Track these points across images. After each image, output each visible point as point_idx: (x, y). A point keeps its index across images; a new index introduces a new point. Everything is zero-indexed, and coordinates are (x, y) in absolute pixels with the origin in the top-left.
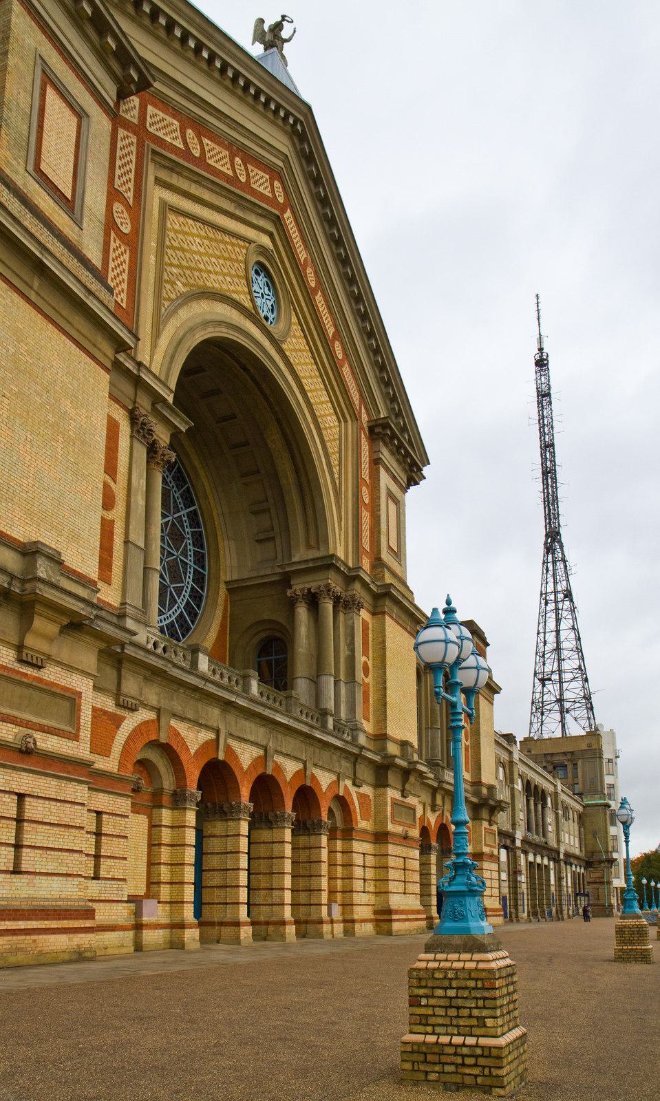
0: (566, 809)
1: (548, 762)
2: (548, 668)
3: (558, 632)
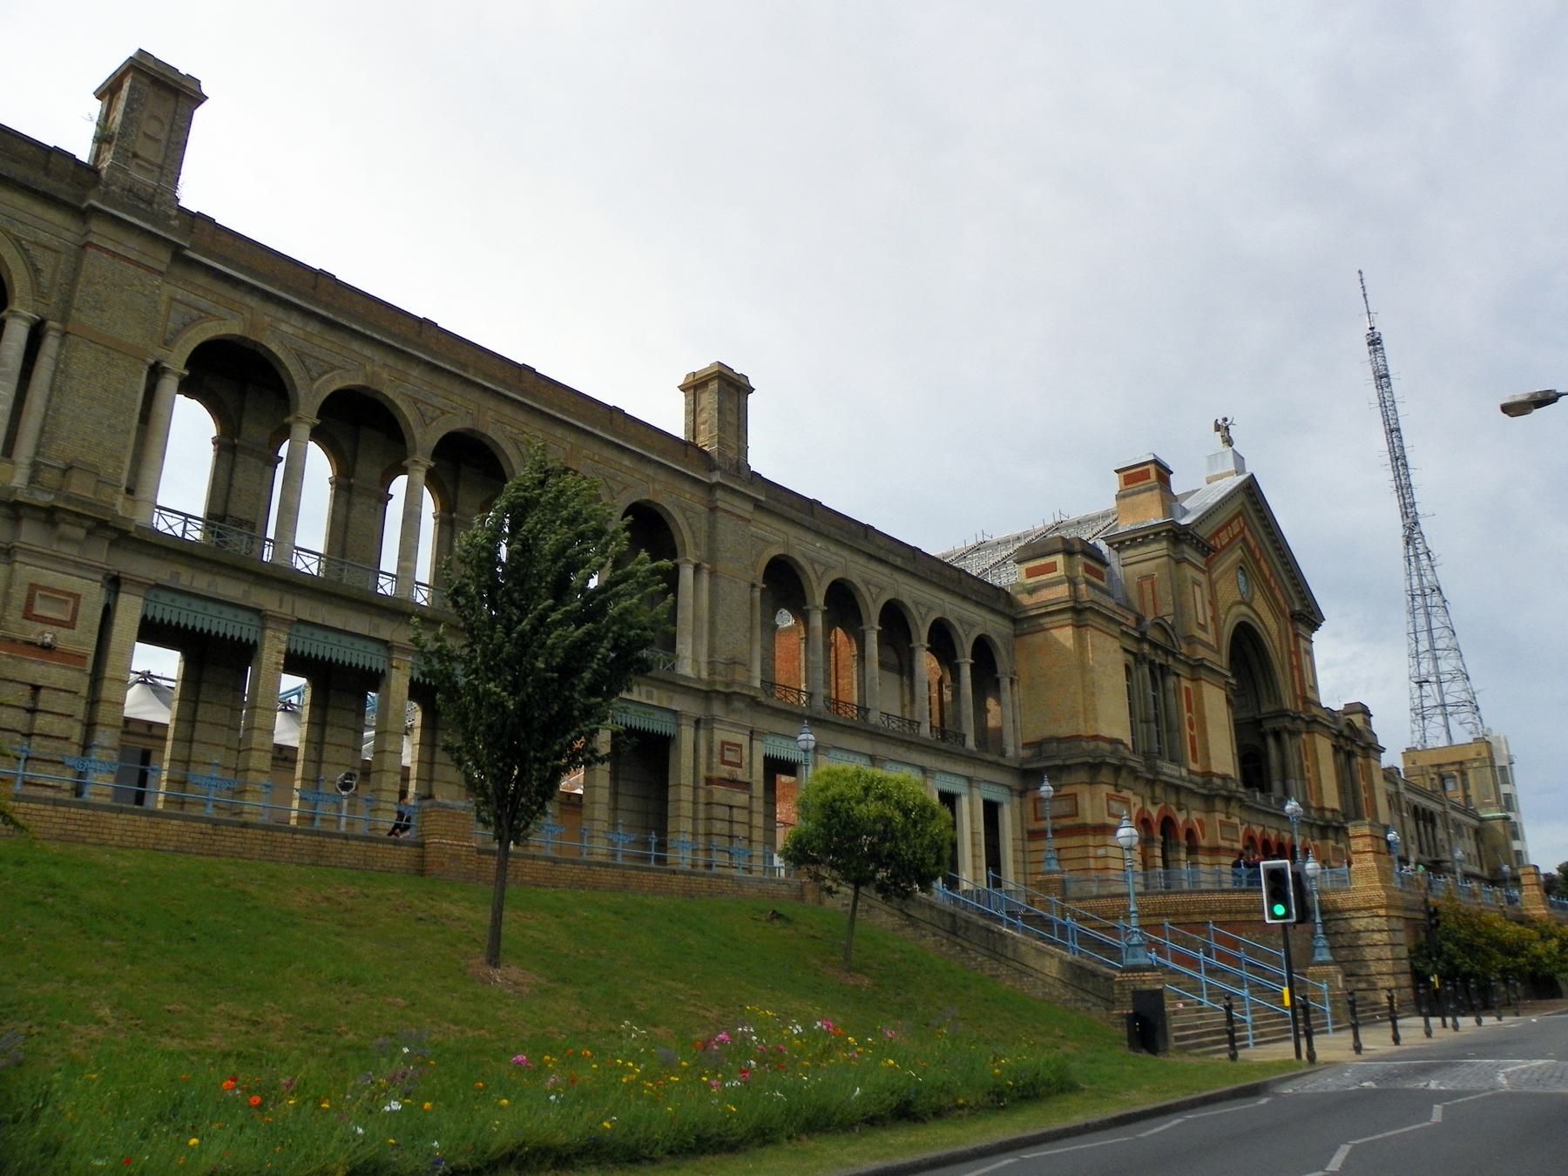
3: (1430, 630)
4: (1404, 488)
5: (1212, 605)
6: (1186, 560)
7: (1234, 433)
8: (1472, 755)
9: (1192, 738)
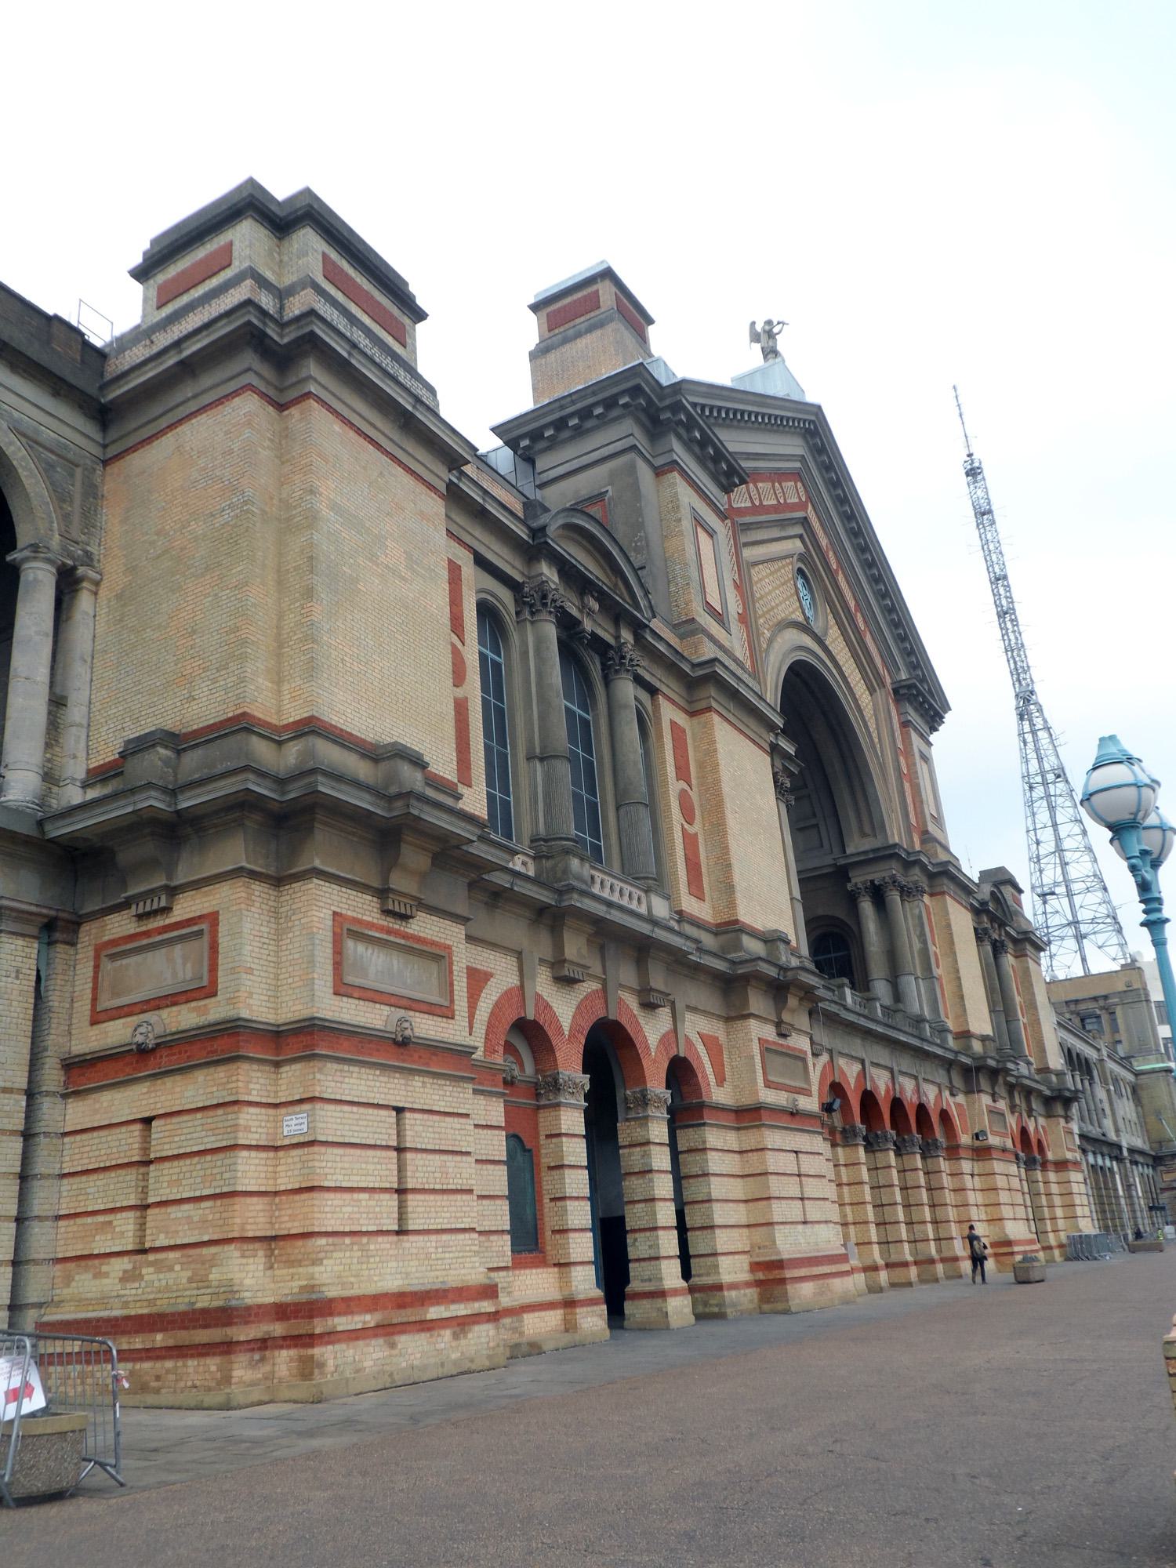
0: (1116, 1081)
1: (1072, 1013)
3: (1055, 825)
4: (1014, 650)
6: (673, 465)
7: (781, 344)
8: (1121, 987)
9: (690, 841)
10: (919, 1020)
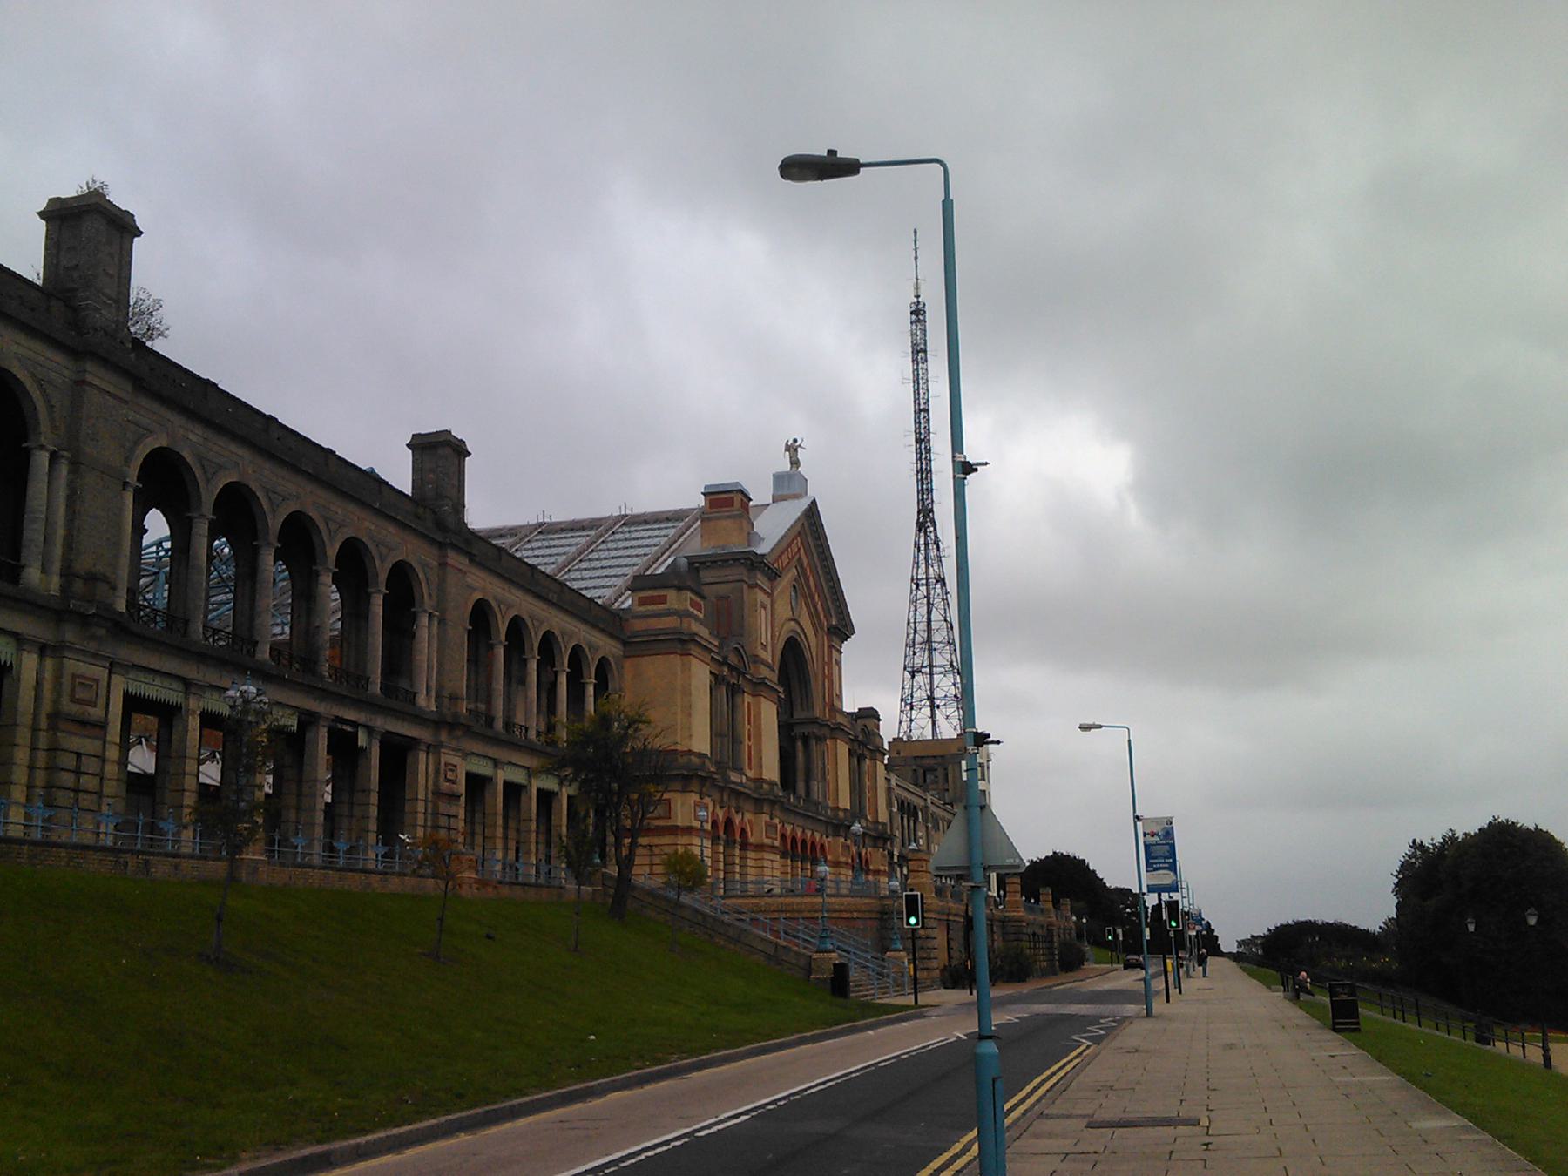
2: (918, 661)
5: (770, 620)
6: (757, 586)
7: (801, 454)
10: (817, 804)
